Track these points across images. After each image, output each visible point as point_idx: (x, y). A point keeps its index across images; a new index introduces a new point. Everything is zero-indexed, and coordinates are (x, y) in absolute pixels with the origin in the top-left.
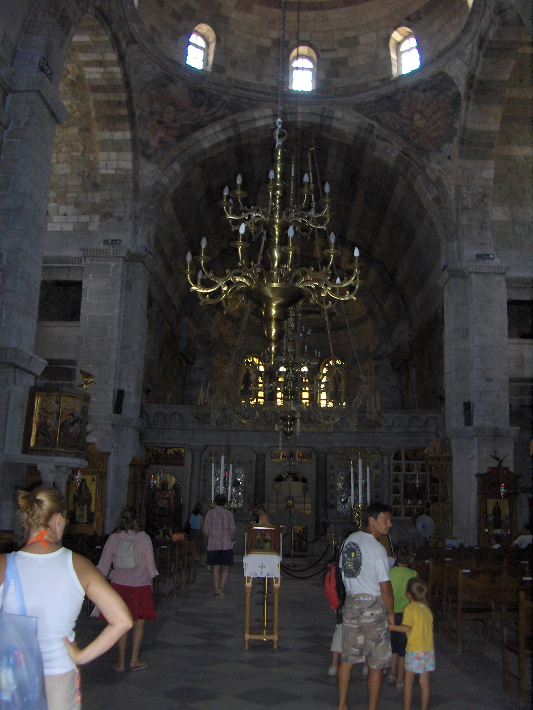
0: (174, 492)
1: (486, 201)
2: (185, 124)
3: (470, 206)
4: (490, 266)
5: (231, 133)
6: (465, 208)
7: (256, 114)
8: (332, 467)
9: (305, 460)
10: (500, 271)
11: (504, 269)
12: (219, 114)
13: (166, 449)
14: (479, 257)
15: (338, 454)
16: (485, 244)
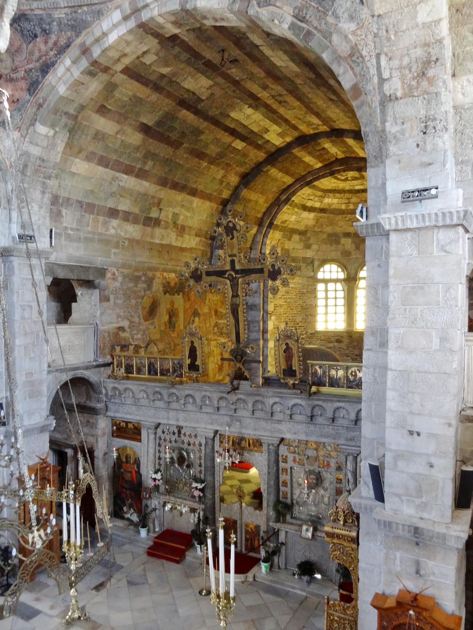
0: (136, 466)
1: (431, 73)
2: (31, 70)
3: (399, 94)
4: (423, 216)
5: (84, 63)
6: (392, 98)
7: (105, 25)
8: (285, 461)
9: (256, 448)
10: (448, 222)
11: (455, 218)
12: (63, 41)
13: (127, 423)
14: (408, 197)
15: (292, 446)
16: (430, 164)
